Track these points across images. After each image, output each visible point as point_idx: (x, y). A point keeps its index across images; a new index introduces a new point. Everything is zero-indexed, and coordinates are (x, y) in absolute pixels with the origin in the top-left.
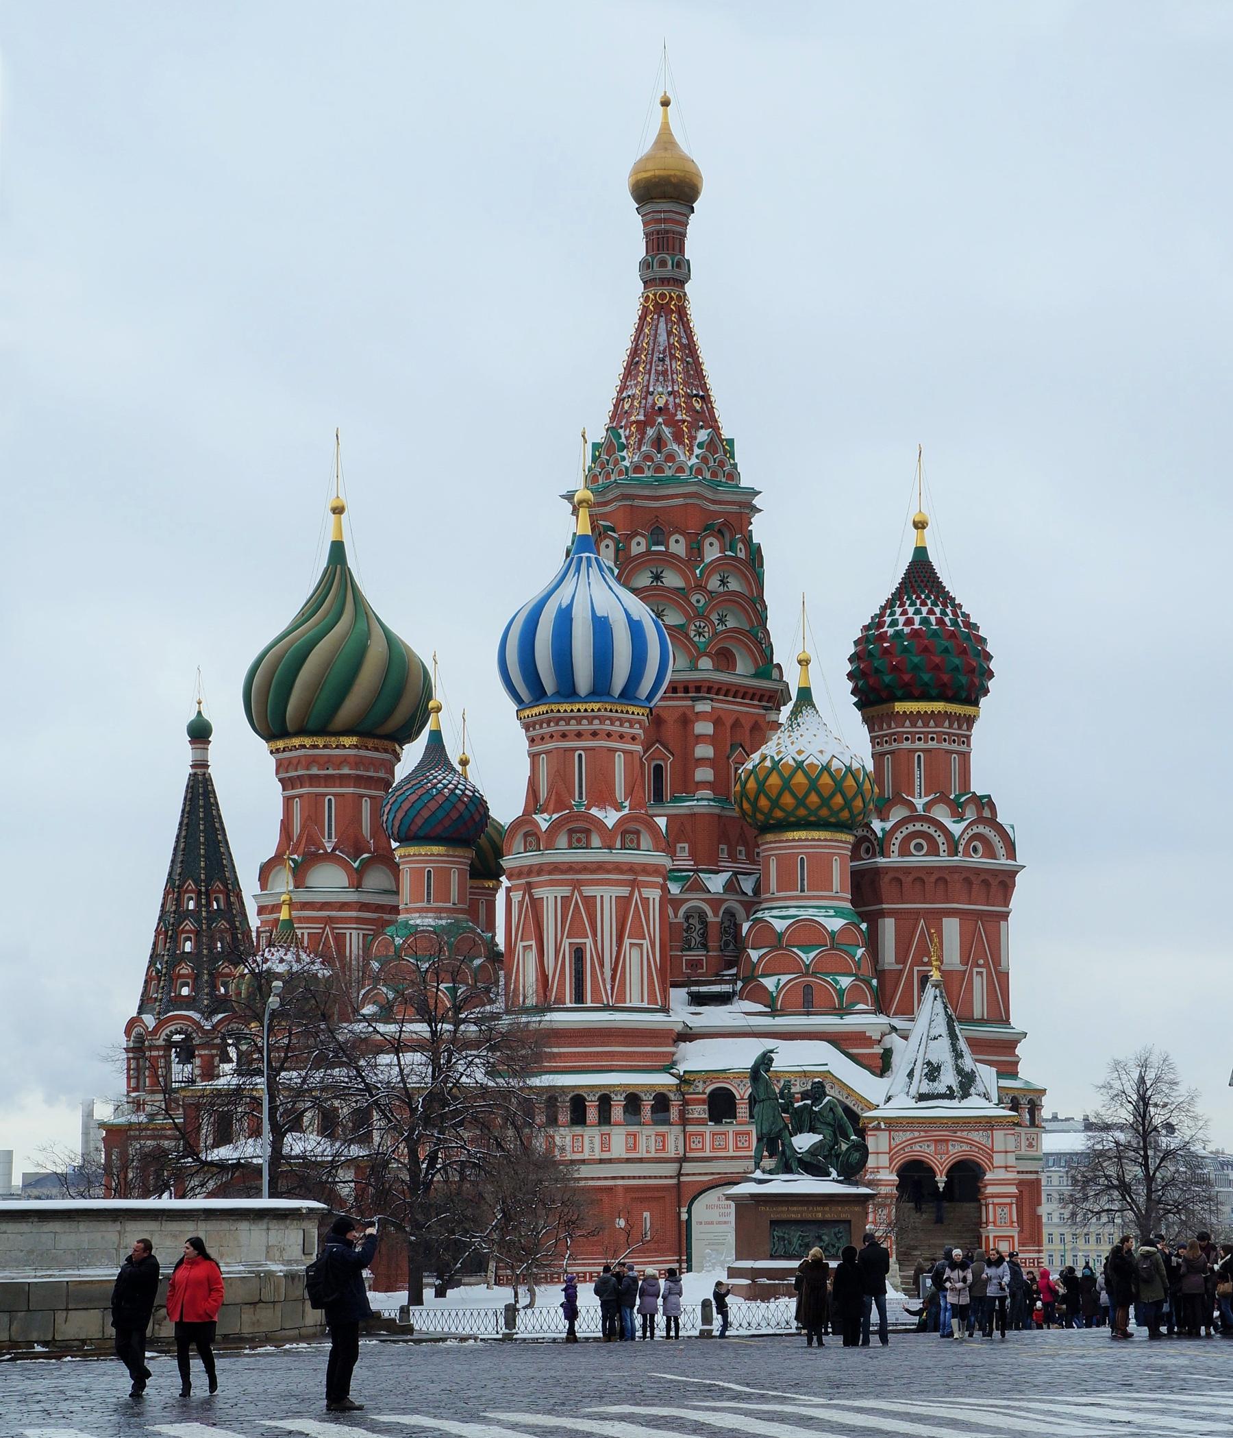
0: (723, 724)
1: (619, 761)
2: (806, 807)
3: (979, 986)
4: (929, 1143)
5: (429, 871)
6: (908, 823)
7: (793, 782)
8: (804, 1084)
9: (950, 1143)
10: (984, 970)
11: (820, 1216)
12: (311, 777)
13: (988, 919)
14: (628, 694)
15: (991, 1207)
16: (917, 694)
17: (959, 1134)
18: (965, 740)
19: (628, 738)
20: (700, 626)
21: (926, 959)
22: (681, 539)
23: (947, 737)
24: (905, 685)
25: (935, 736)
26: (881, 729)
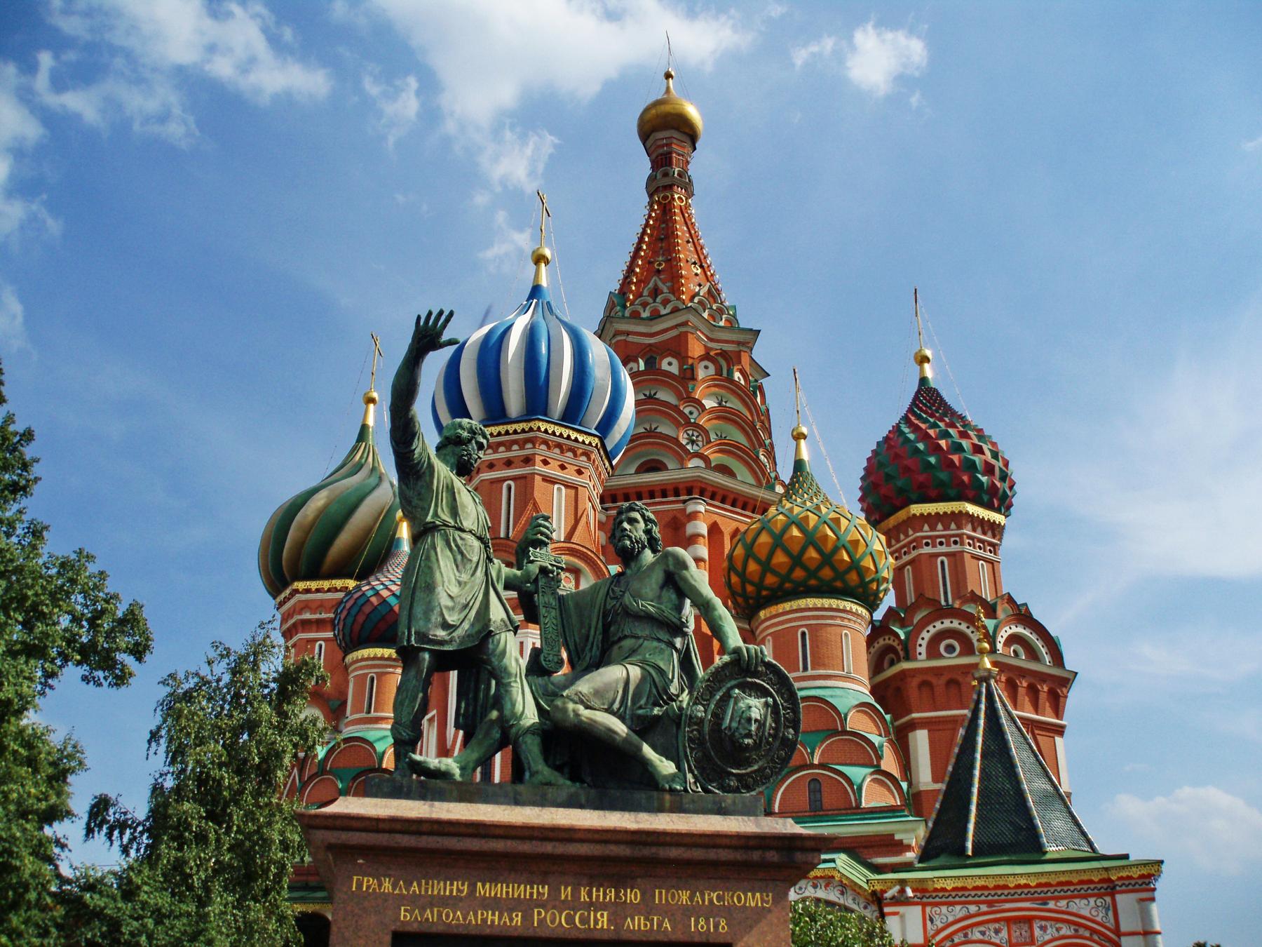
0: (721, 533)
2: (805, 568)
4: (997, 925)
5: (372, 679)
6: (936, 620)
7: (786, 536)
8: (800, 888)
9: (1036, 925)
11: (602, 920)
13: (1041, 733)
17: (1051, 905)
19: (571, 469)
20: (693, 435)
22: (675, 362)
23: (971, 542)
24: (921, 486)
25: (958, 539)
26: (898, 541)
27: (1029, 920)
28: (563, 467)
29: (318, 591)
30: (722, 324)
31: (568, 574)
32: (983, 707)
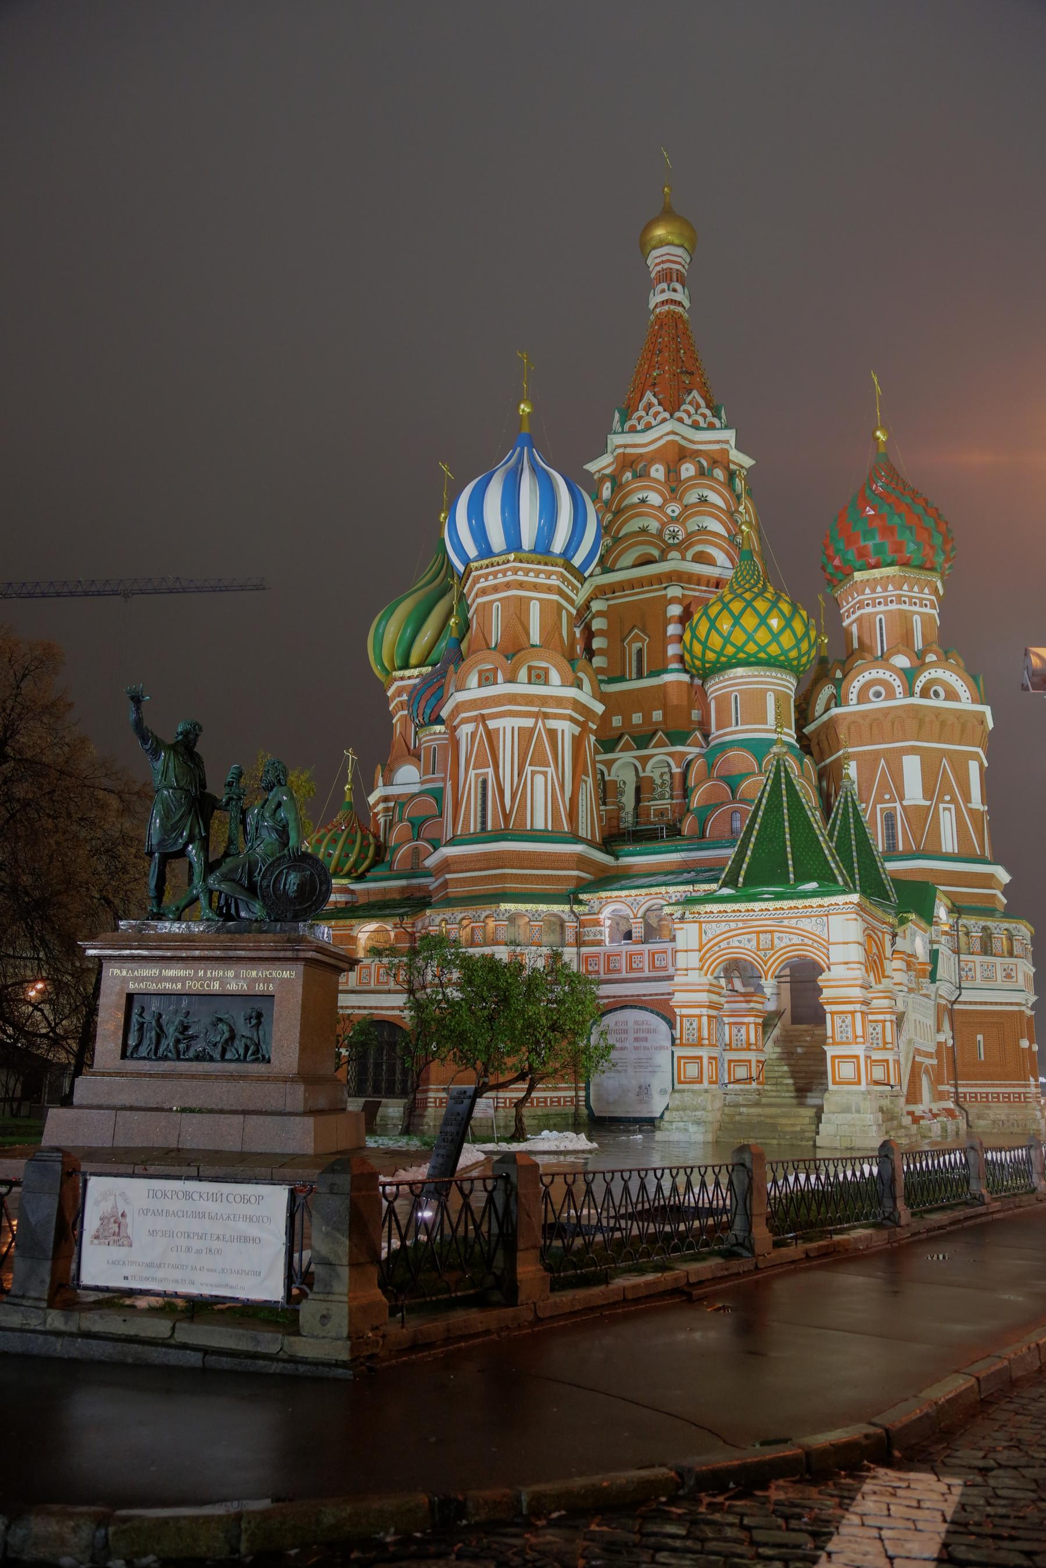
1: (535, 608)
2: (733, 645)
3: (947, 822)
4: (749, 936)
9: (776, 935)
10: (952, 807)
11: (216, 987)
12: (401, 702)
14: (542, 550)
15: (828, 1017)
16: (872, 561)
17: (786, 922)
18: (928, 603)
21: (887, 797)
26: (848, 603)
27: (771, 932)
28: (536, 587)
29: (409, 678)
30: (705, 426)
31: (538, 672)
32: (772, 776)
